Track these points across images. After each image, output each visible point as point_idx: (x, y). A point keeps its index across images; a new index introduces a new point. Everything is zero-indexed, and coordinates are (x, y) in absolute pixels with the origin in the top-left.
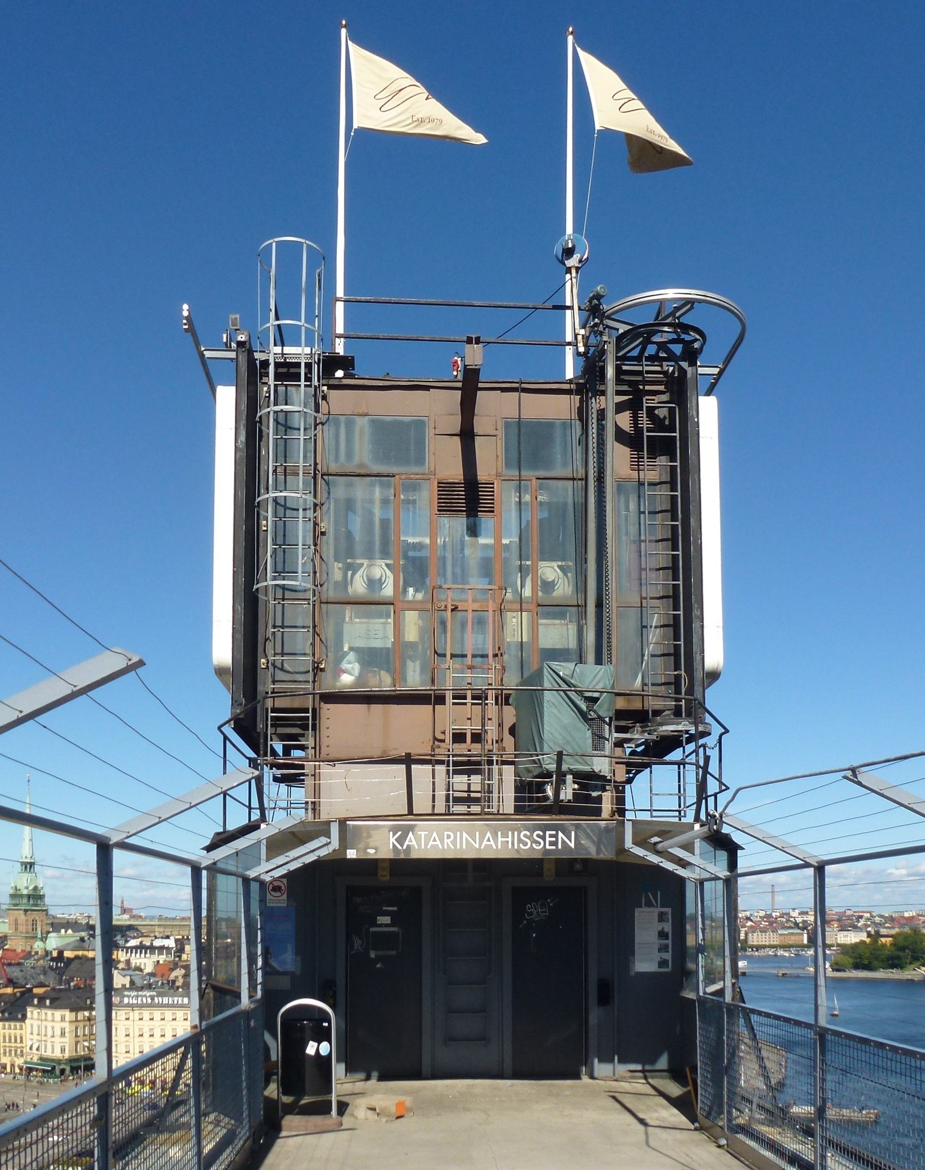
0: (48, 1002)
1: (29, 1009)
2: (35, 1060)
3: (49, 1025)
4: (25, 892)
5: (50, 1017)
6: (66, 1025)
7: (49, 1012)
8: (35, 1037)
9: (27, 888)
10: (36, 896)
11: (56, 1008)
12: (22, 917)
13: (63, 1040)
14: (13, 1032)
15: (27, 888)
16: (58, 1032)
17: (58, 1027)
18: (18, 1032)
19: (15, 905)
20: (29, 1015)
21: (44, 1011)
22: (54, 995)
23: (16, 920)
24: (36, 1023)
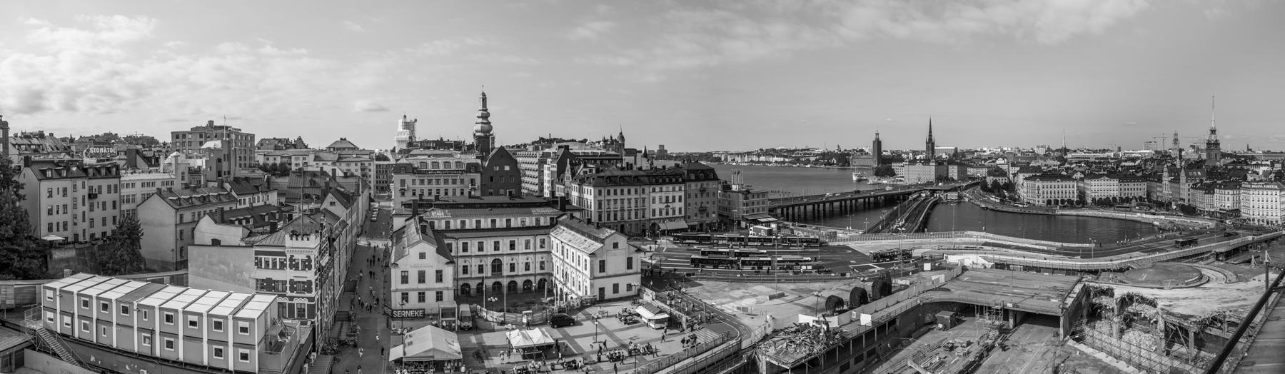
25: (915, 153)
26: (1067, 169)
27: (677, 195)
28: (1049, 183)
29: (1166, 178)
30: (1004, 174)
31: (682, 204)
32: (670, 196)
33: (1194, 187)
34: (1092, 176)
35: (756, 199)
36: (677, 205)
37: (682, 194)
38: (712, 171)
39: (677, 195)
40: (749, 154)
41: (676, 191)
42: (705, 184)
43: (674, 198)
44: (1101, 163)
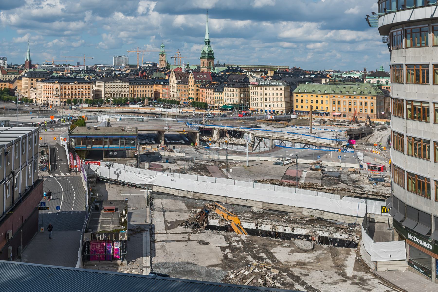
0: (231, 85)
1: (224, 88)
2: (227, 104)
3: (232, 93)
4: (207, 52)
5: (232, 90)
6: (238, 93)
7: (232, 89)
8: (227, 97)
9: (208, 50)
10: (211, 54)
11: (234, 87)
12: (206, 61)
13: (237, 98)
14: (219, 96)
15: (208, 50)
16: (235, 96)
17: (235, 93)
18: (221, 96)
19: (203, 57)
20: (224, 90)
21: (230, 89)
22: (233, 83)
23: (204, 62)
24: (227, 93)
28: (67, 86)
29: (173, 79)
33: (204, 86)
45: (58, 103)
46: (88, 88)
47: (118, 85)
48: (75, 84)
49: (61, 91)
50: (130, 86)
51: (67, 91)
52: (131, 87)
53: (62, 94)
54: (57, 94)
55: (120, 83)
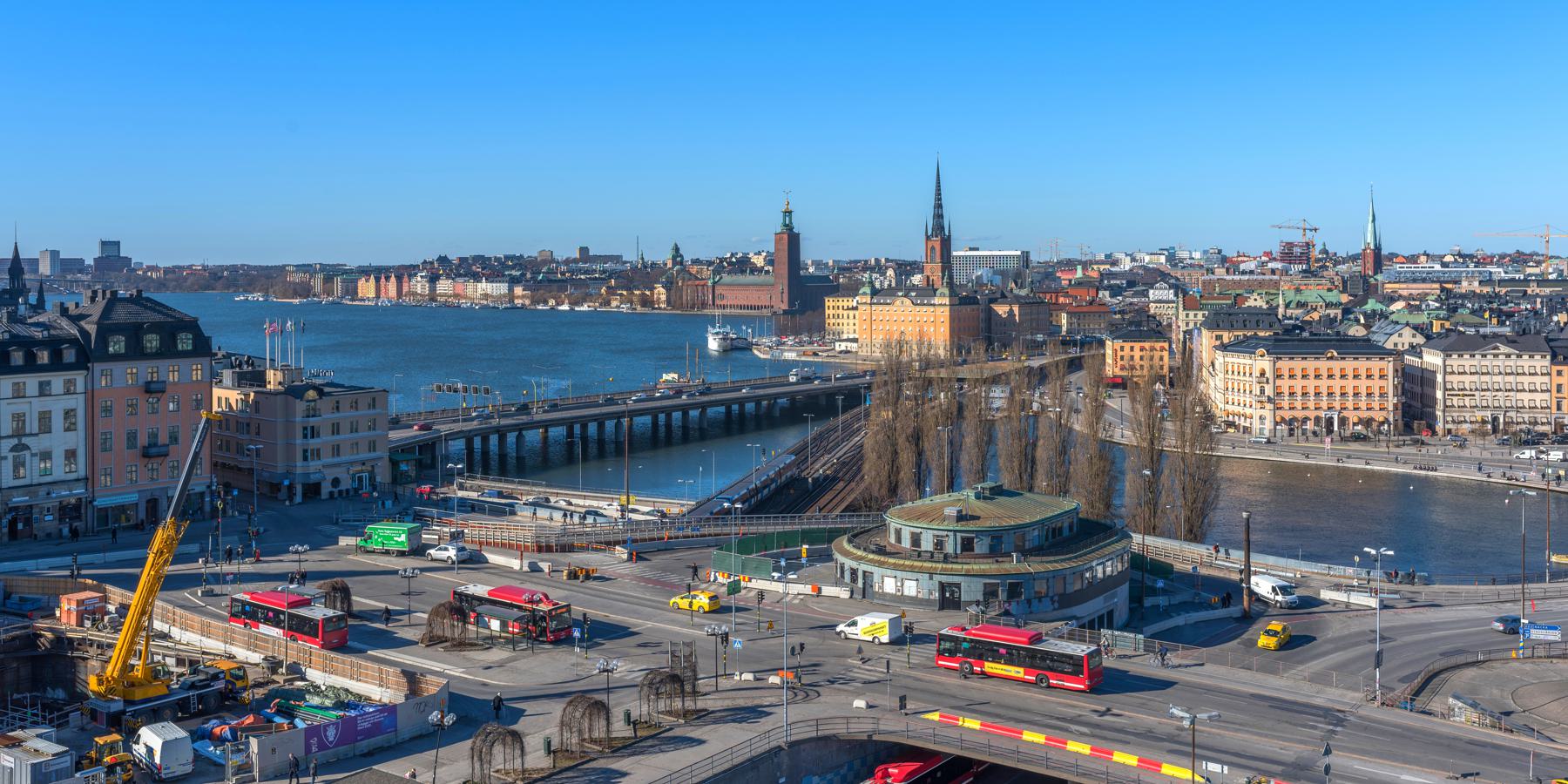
25: (905, 269)
26: (1371, 317)
27: (57, 407)
30: (1156, 330)
31: (77, 440)
32: (32, 408)
34: (1453, 343)
35: (346, 414)
36: (59, 440)
37: (78, 402)
38: (192, 326)
39: (57, 407)
40: (404, 273)
41: (62, 394)
42: (171, 371)
43: (45, 419)
44: (1493, 305)
45: (1269, 425)
46: (1377, 376)
47: (1501, 362)
48: (1331, 358)
49: (1278, 382)
50: (1555, 368)
51: (1298, 384)
52: (1559, 373)
53: (1279, 394)
54: (1262, 391)
55: (1508, 356)
